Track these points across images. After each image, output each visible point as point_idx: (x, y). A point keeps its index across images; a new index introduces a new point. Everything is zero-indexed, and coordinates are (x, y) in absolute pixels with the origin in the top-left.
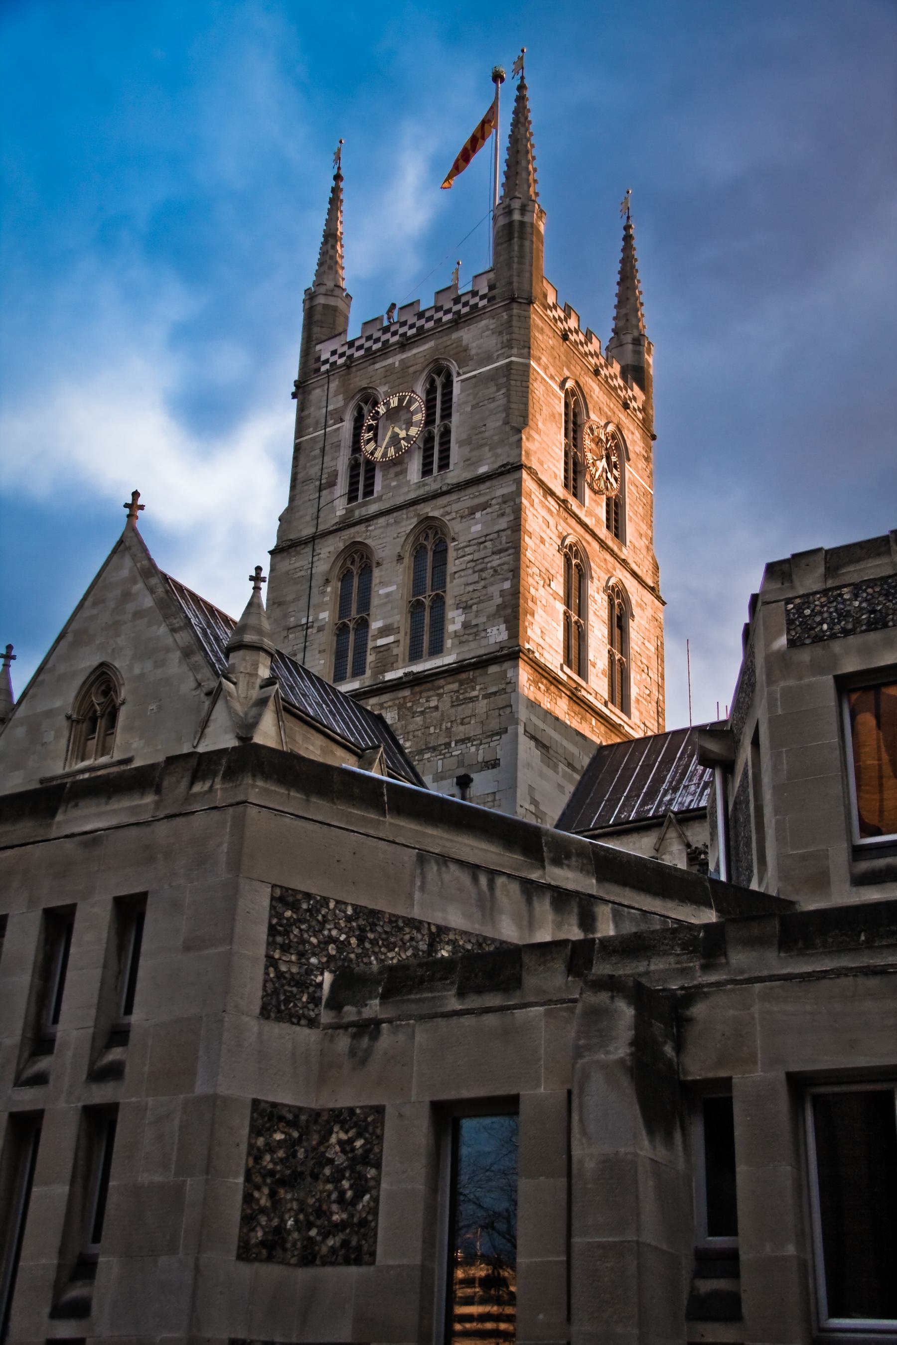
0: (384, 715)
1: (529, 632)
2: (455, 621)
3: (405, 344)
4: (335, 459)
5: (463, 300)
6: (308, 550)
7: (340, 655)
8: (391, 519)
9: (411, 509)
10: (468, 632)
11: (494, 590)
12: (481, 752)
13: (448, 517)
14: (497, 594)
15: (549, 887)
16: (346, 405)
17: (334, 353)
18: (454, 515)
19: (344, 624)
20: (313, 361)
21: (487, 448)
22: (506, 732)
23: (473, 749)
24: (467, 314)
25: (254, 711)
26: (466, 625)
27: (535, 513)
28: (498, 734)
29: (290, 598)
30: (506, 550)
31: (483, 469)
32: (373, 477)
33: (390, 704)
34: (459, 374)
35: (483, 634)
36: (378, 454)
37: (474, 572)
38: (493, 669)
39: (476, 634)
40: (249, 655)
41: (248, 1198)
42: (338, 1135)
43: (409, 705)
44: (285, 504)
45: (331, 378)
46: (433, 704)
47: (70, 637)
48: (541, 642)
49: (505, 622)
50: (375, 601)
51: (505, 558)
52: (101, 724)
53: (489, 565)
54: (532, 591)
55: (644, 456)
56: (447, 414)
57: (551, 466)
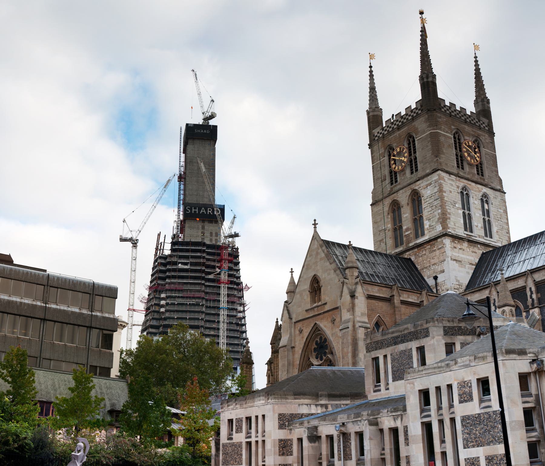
0: (411, 258)
1: (449, 225)
2: (427, 224)
3: (399, 128)
4: (384, 171)
5: (414, 111)
6: (381, 203)
7: (396, 238)
8: (403, 190)
9: (409, 187)
10: (431, 228)
11: (436, 213)
12: (439, 268)
13: (420, 189)
14: (437, 215)
15: (320, 404)
16: (385, 151)
17: (378, 133)
18: (422, 188)
19: (396, 228)
20: (372, 136)
21: (428, 164)
22: (445, 260)
23: (437, 267)
24: (415, 116)
25: (354, 287)
26: (430, 226)
27: (446, 183)
28: (443, 261)
29: (379, 220)
30: (438, 199)
31: (428, 171)
32: (397, 176)
33: (412, 254)
34: (416, 138)
35: (435, 228)
36: (396, 168)
37: (430, 207)
38: (439, 240)
39: (433, 228)
40: (351, 270)
41: (279, 450)
42: (289, 442)
43: (417, 254)
44: (373, 188)
45: (379, 142)
46: (424, 253)
47: (305, 267)
48: (454, 227)
49: (441, 224)
50: (403, 220)
51: (438, 202)
52: (318, 292)
53: (434, 204)
54: (449, 211)
55: (491, 142)
56: (415, 152)
57: (451, 164)
